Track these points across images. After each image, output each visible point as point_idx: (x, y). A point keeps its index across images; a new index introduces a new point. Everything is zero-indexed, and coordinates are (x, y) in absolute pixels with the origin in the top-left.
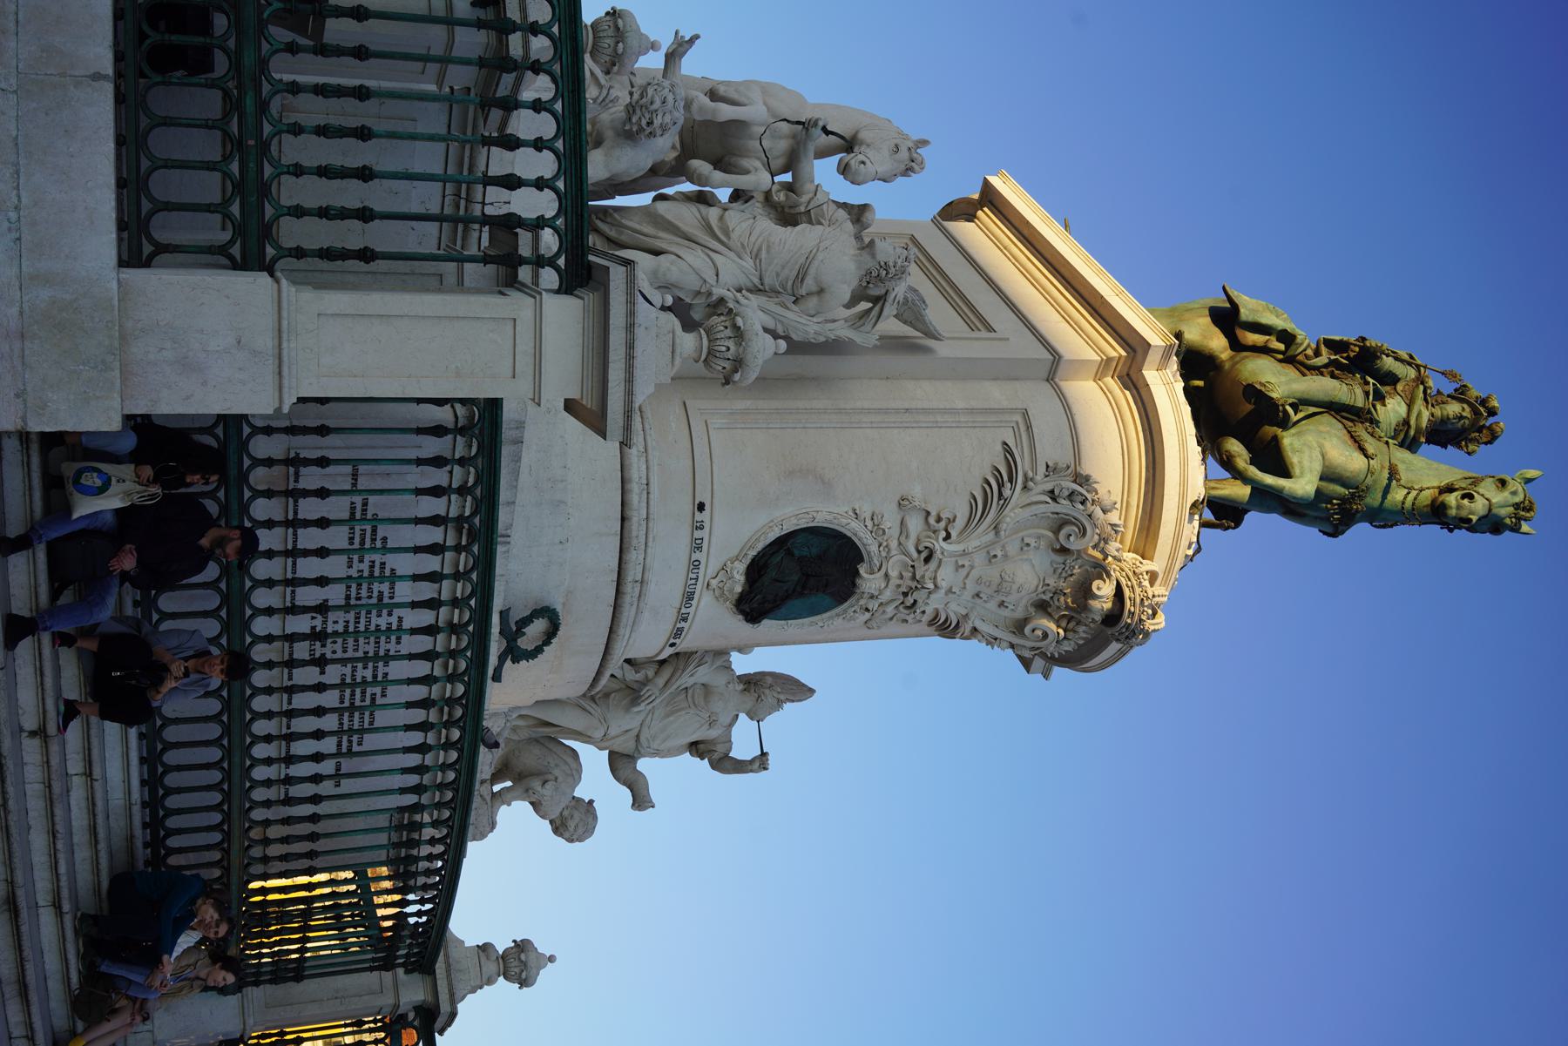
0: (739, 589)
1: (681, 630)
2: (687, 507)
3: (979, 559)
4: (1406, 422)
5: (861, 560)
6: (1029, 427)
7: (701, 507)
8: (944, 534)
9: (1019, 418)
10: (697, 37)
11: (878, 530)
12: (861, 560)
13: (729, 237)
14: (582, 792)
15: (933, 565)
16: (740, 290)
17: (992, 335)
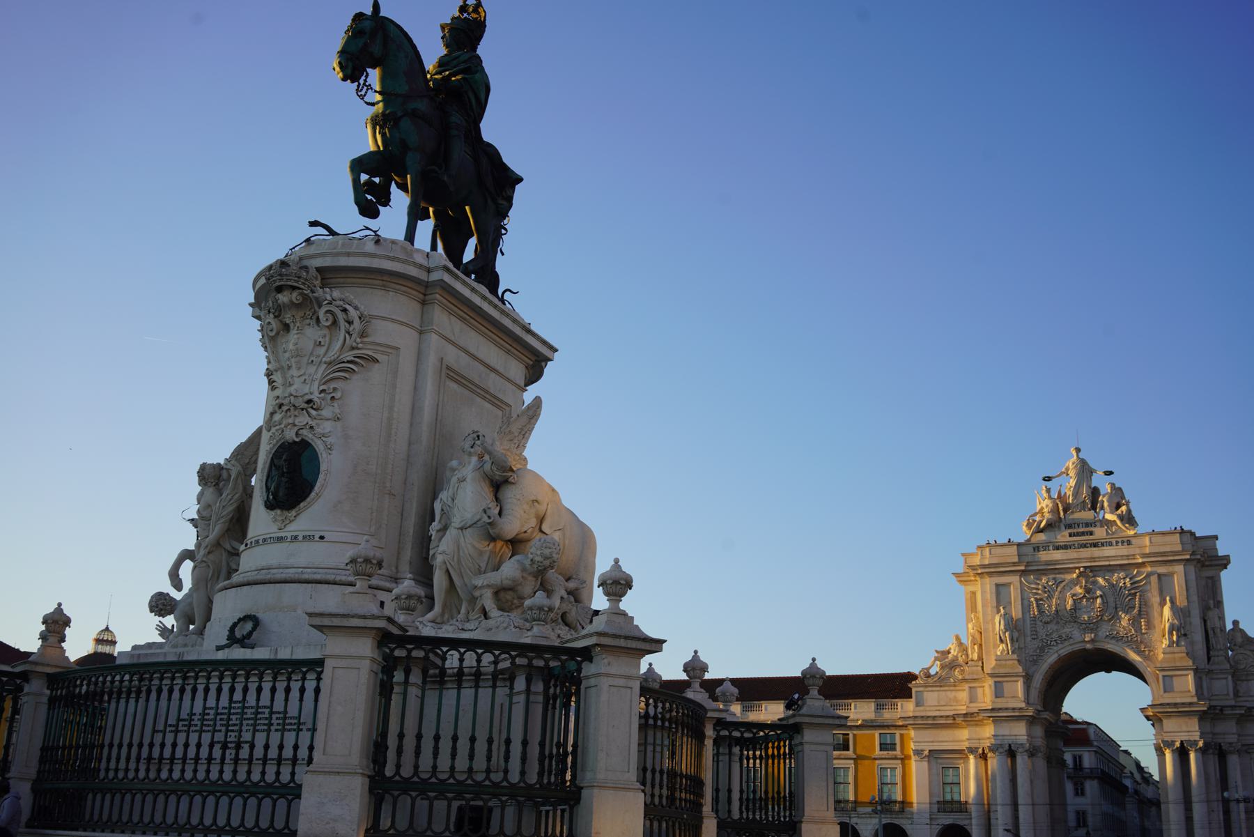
0: (279, 512)
1: (305, 537)
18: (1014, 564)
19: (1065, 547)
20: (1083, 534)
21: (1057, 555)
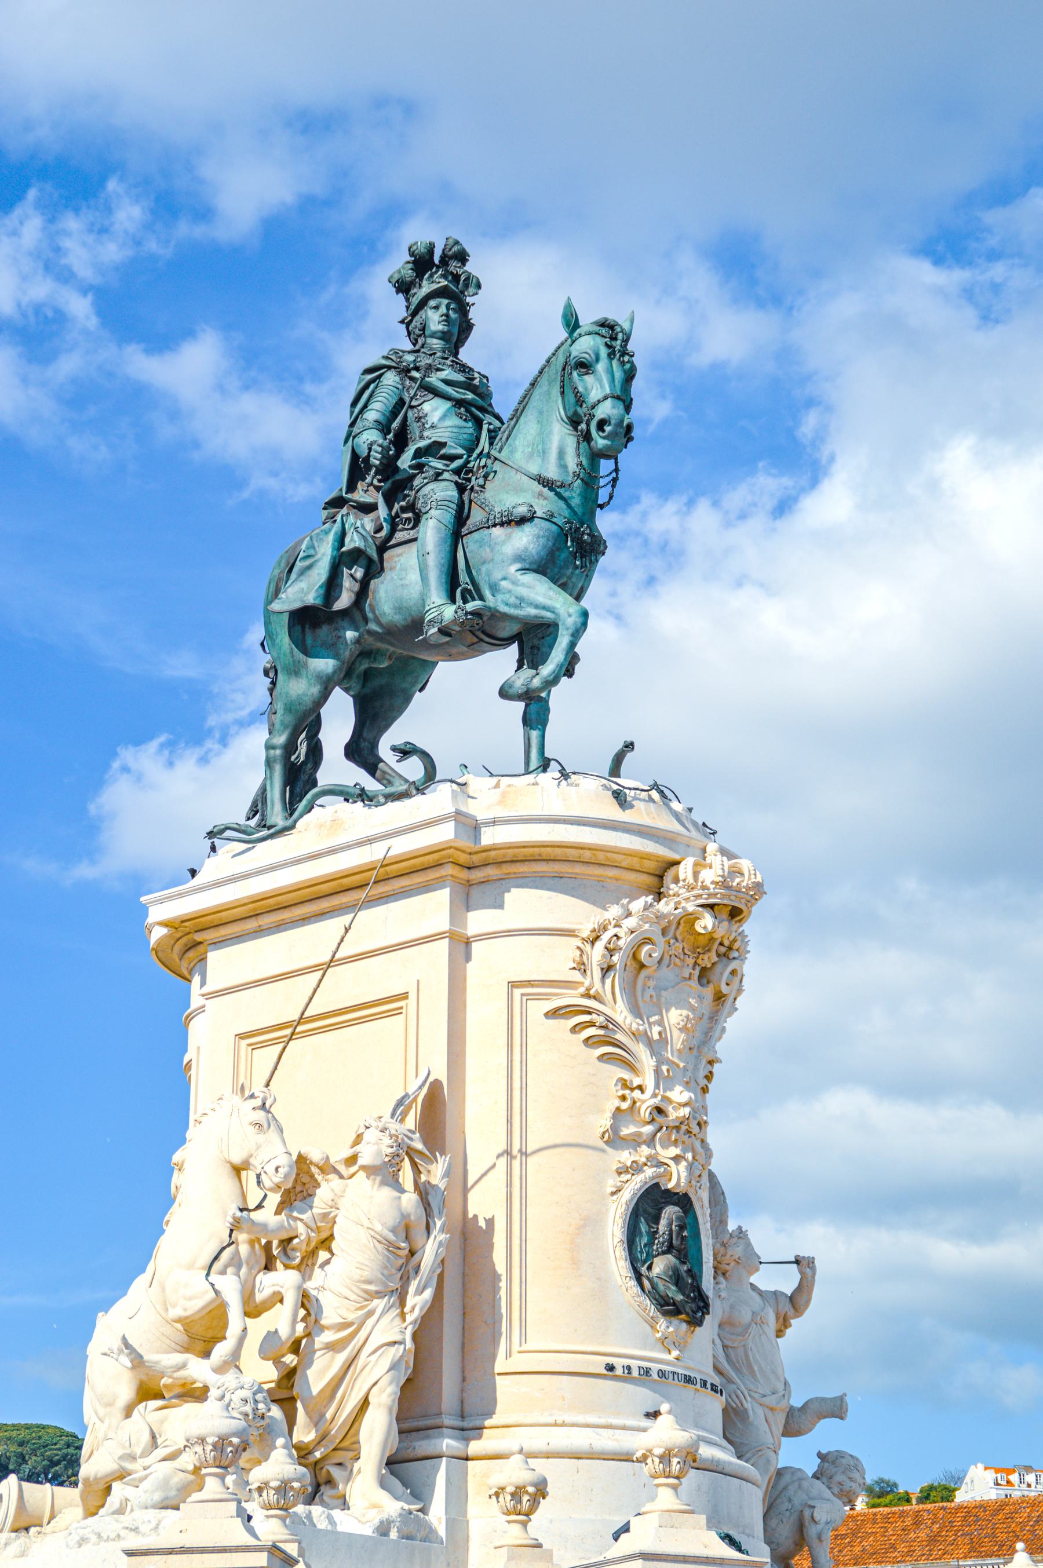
4: (459, 403)
5: (657, 1185)
6: (530, 983)
7: (611, 1368)
8: (637, 1094)
9: (517, 992)
10: (124, 1338)
12: (657, 1185)
13: (349, 1325)
14: (811, 1466)
16: (403, 1316)
17: (412, 996)
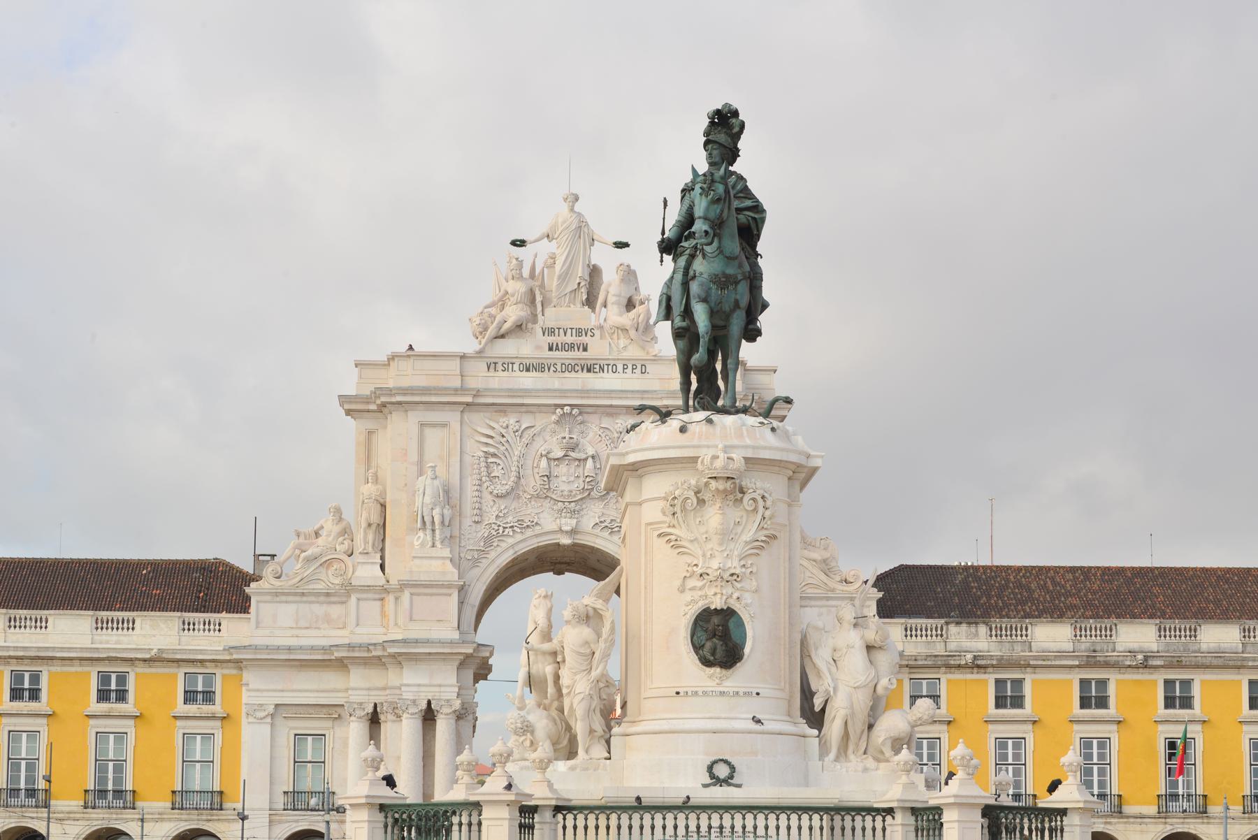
0: (718, 670)
1: (745, 693)
2: (678, 699)
3: (709, 546)
11: (694, 601)
15: (709, 571)
18: (456, 391)
19: (540, 368)
20: (572, 347)
21: (528, 381)
